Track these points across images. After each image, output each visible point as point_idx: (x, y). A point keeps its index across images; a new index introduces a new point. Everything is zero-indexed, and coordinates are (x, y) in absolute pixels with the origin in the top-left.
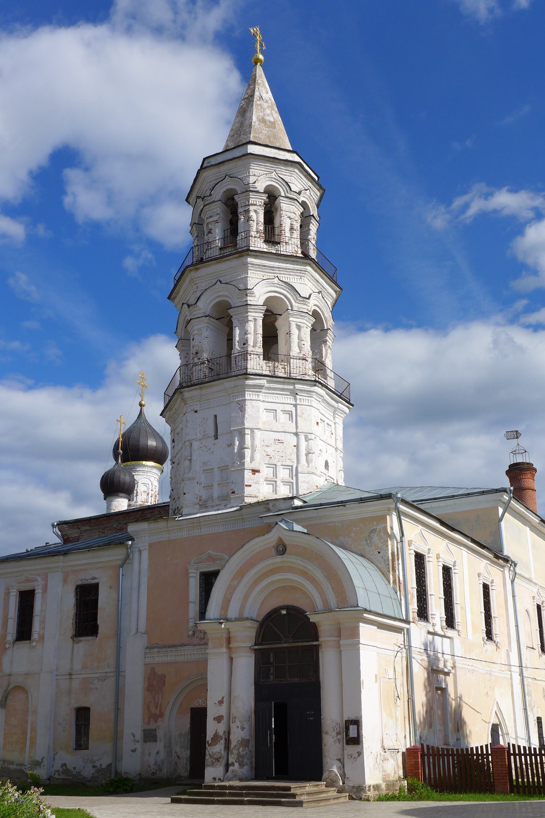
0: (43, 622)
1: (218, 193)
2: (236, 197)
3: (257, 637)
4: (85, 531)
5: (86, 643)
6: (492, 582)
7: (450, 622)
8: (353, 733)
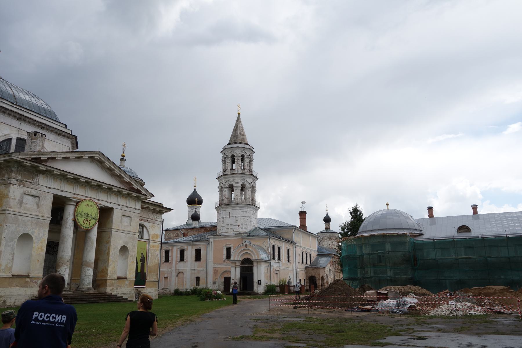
0: (187, 257)
1: (230, 156)
2: (234, 157)
3: (241, 263)
4: (189, 231)
5: (198, 263)
6: (290, 248)
7: (279, 259)
8: (260, 283)
